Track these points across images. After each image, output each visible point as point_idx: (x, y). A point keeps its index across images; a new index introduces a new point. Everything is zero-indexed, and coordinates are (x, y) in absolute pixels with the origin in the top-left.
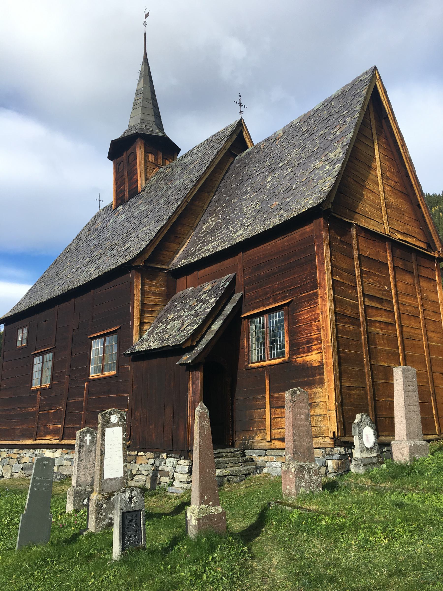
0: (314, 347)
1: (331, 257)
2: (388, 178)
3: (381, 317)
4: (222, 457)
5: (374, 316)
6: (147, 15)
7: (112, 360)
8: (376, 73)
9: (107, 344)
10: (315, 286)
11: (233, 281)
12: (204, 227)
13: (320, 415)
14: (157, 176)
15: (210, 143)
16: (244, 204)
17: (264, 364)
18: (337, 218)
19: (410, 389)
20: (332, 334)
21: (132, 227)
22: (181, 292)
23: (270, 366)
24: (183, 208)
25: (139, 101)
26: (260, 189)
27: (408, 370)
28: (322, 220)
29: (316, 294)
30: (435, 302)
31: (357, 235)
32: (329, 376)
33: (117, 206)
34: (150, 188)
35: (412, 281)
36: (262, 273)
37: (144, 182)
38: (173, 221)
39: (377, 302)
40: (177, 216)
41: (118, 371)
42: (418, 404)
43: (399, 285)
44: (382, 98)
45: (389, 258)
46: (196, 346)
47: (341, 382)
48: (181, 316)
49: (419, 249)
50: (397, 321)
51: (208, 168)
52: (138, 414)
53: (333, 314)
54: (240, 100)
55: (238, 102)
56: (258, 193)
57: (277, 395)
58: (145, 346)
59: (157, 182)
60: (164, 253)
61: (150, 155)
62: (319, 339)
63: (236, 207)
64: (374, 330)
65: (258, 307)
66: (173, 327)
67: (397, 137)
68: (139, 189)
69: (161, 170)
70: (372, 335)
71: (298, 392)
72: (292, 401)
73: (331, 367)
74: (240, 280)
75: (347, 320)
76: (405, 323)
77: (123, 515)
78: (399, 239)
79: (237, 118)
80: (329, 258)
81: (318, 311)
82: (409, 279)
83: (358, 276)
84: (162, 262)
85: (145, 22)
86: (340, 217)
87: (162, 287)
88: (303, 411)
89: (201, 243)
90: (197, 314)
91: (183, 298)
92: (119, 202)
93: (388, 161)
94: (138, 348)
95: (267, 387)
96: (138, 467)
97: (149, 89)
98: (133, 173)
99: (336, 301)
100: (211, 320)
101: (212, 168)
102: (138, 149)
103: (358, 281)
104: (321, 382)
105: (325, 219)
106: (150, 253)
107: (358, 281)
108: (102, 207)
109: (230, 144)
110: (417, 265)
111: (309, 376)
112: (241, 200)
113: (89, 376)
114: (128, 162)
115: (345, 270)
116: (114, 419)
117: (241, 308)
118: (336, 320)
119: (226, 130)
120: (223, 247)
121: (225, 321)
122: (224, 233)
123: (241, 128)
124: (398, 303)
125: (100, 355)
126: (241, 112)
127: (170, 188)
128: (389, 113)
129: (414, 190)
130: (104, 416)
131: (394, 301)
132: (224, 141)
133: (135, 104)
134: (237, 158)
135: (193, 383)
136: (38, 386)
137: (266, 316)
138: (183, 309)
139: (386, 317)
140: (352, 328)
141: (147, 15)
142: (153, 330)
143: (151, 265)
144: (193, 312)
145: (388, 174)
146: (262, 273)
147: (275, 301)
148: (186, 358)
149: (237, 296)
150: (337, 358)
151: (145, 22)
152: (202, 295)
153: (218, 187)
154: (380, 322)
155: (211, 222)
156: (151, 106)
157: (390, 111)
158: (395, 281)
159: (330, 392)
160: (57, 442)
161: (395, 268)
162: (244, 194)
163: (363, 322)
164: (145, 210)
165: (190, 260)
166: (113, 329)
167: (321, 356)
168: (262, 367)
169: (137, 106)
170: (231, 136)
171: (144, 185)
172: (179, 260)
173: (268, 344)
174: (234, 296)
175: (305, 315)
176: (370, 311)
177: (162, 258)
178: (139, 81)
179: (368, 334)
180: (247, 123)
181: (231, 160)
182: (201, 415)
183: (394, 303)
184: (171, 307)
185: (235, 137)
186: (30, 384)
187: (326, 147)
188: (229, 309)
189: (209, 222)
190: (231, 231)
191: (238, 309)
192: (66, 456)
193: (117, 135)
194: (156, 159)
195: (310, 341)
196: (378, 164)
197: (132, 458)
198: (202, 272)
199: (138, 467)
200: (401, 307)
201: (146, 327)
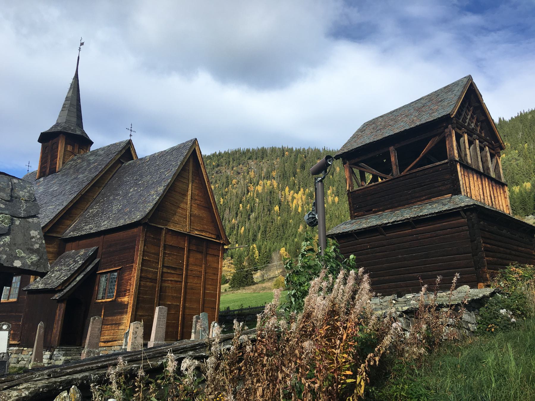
1: (144, 246)
2: (196, 200)
4: (71, 351)
5: (168, 277)
10: (133, 262)
15: (108, 150)
16: (115, 202)
17: (103, 301)
19: (162, 317)
23: (106, 302)
25: (67, 106)
26: (125, 195)
27: (163, 308)
29: (132, 266)
31: (165, 233)
32: (130, 310)
33: (40, 178)
35: (201, 257)
37: (61, 165)
38: (69, 207)
40: (72, 204)
41: (18, 298)
43: (191, 260)
47: (136, 312)
51: (100, 172)
52: (26, 326)
57: (106, 318)
58: (36, 286)
59: (70, 168)
61: (69, 146)
62: (129, 290)
64: (166, 285)
68: (57, 169)
69: (75, 158)
72: (93, 322)
73: (131, 305)
75: (148, 280)
76: (190, 280)
79: (129, 138)
82: (199, 256)
84: (57, 232)
88: (98, 327)
90: (70, 270)
91: (68, 257)
92: (42, 174)
93: (198, 190)
94: (32, 287)
96: (23, 356)
97: (75, 97)
99: (142, 271)
103: (161, 259)
104: (126, 312)
106: (49, 227)
107: (161, 259)
108: (30, 172)
112: (114, 199)
115: (153, 253)
116: (5, 327)
118: (140, 281)
119: (120, 143)
126: (131, 135)
127: (75, 178)
132: (115, 154)
133: (64, 107)
135: (60, 310)
137: (109, 274)
138: (64, 265)
141: (82, 44)
143: (52, 235)
144: (68, 268)
145: (196, 198)
147: (115, 267)
153: (106, 184)
154: (171, 281)
155: (95, 209)
156: (75, 110)
158: (188, 257)
161: (189, 251)
162: (118, 195)
164: (56, 190)
165: (76, 234)
167: (128, 299)
168: (102, 302)
170: (121, 151)
171: (61, 167)
172: (70, 233)
176: (165, 275)
177: (58, 230)
178: (69, 91)
179: (161, 287)
181: (120, 165)
182: (40, 327)
187: (159, 183)
190: (102, 220)
191: (96, 267)
193: (47, 127)
194: (73, 149)
195: (126, 291)
198: (81, 242)
199: (23, 356)
200: (189, 272)
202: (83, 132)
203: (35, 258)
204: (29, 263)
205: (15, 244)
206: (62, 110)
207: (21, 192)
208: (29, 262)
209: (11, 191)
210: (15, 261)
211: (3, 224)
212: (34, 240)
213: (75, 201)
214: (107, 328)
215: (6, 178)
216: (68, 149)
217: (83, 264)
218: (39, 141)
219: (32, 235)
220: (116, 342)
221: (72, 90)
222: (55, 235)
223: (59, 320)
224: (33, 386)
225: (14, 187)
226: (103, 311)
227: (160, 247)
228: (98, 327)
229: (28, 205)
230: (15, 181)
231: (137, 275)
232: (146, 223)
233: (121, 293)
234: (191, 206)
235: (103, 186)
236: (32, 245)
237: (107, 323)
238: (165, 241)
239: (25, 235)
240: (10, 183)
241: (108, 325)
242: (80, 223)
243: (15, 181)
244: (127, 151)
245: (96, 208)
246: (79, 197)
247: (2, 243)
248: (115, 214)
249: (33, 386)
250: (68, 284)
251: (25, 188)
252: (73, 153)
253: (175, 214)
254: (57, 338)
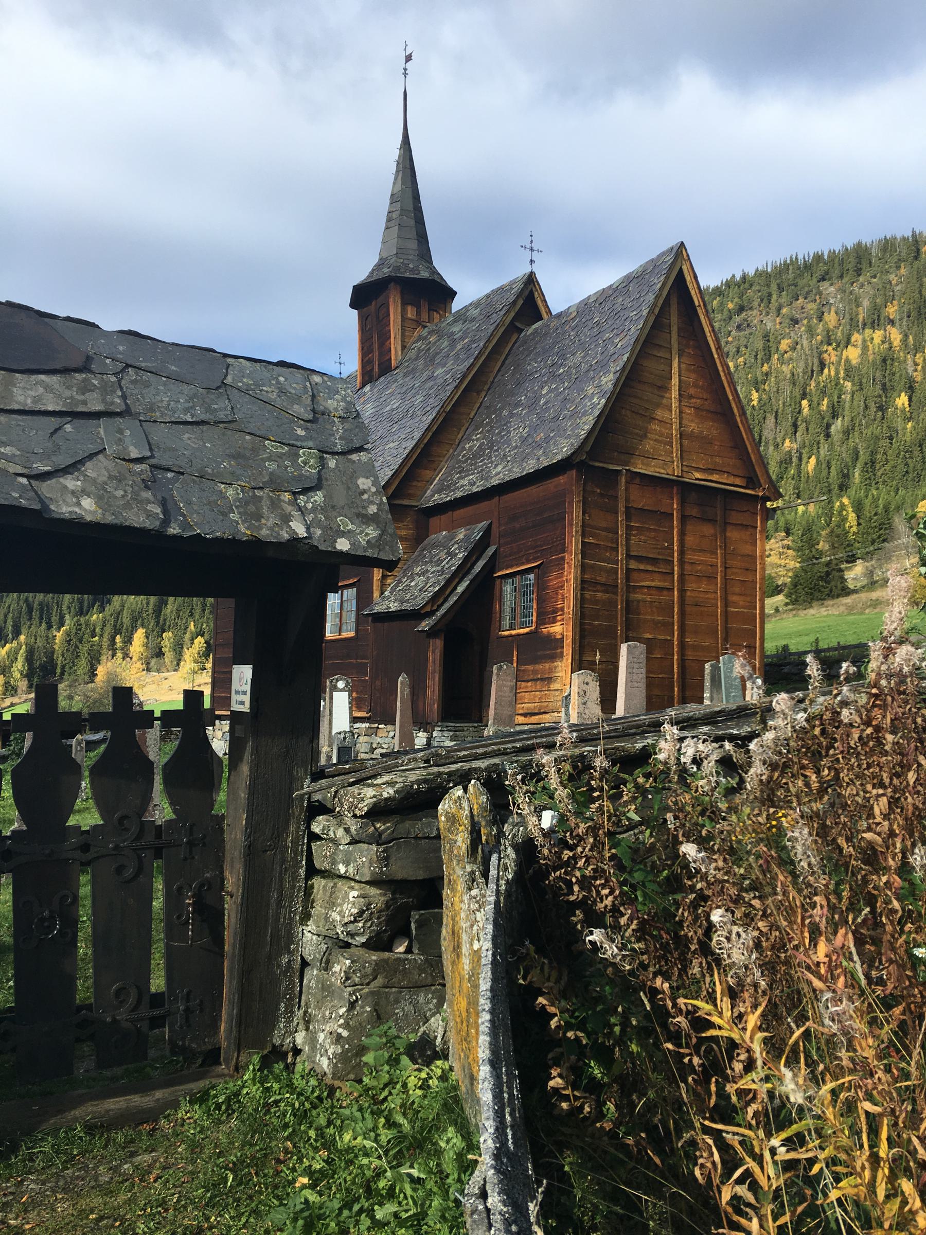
1: (583, 514)
2: (691, 397)
3: (653, 581)
4: (463, 731)
6: (408, 58)
7: (351, 618)
8: (684, 252)
9: (345, 598)
11: (488, 532)
12: (467, 446)
13: (557, 690)
14: (418, 344)
16: (514, 423)
17: (513, 632)
18: (599, 467)
19: (636, 666)
20: (575, 605)
21: (379, 434)
22: (433, 536)
23: (519, 635)
24: (439, 422)
25: (394, 215)
26: (533, 404)
27: (636, 647)
28: (574, 472)
29: (563, 558)
30: (748, 555)
31: (626, 482)
32: (568, 650)
33: (363, 385)
34: (408, 367)
35: (712, 531)
37: (400, 353)
38: (425, 441)
39: (648, 564)
40: (430, 434)
41: (357, 631)
42: (644, 680)
43: (690, 540)
44: (690, 287)
45: (675, 506)
46: (437, 610)
47: (581, 655)
48: (427, 571)
49: (732, 488)
50: (676, 584)
51: (477, 358)
52: (378, 683)
53: (579, 582)
54: (532, 242)
55: (528, 246)
56: (532, 408)
57: (523, 668)
58: (385, 607)
60: (415, 483)
61: (409, 308)
62: (562, 609)
63: (505, 425)
64: (639, 596)
65: (511, 567)
66: (416, 585)
67: (709, 339)
69: (425, 332)
70: (635, 603)
71: (505, 667)
72: (498, 675)
73: (570, 640)
75: (599, 587)
76: (691, 586)
77: (339, 749)
78: (697, 479)
79: (528, 270)
80: (580, 518)
81: (564, 579)
82: (708, 530)
83: (622, 535)
84: (410, 496)
85: (405, 69)
86: (601, 465)
87: (410, 529)
88: (509, 684)
89: (460, 472)
90: (442, 572)
91: (434, 546)
96: (379, 740)
97: (409, 193)
98: (385, 337)
99: (584, 567)
100: (457, 580)
101: (483, 358)
102: (391, 300)
103: (622, 541)
104: (561, 656)
105: (578, 471)
107: (622, 541)
109: (513, 314)
110: (726, 509)
111: (552, 647)
112: (511, 415)
114: (378, 317)
116: (341, 684)
117: (495, 565)
118: (583, 589)
120: (478, 487)
121: (472, 581)
122: (485, 464)
123: (532, 285)
124: (682, 562)
125: (338, 611)
126: (531, 261)
128: (699, 306)
129: (731, 408)
130: (331, 682)
131: (676, 560)
133: (389, 220)
134: (523, 333)
138: (431, 561)
139: (660, 581)
140: (606, 596)
141: (408, 58)
142: (397, 586)
145: (692, 391)
147: (528, 562)
148: (425, 625)
149: (491, 550)
150: (578, 630)
151: (405, 69)
152: (453, 545)
153: (492, 382)
154: (648, 587)
156: (412, 223)
157: (702, 304)
158: (682, 534)
159: (567, 666)
161: (684, 519)
162: (518, 405)
163: (622, 589)
164: (397, 408)
166: (351, 581)
168: (511, 636)
169: (391, 224)
171: (400, 357)
173: (518, 611)
176: (635, 575)
178: (396, 179)
179: (628, 602)
180: (540, 277)
183: (676, 563)
184: (419, 555)
185: (521, 302)
187: (603, 366)
188: (478, 568)
189: (473, 440)
193: (361, 272)
194: (419, 313)
195: (555, 611)
196: (675, 381)
197: (373, 731)
199: (379, 740)
200: (687, 567)
201: (389, 581)
202: (434, 271)
203: (372, 532)
204: (364, 543)
205: (333, 507)
206: (387, 228)
207: (330, 401)
208: (362, 540)
209: (312, 400)
210: (338, 540)
211: (307, 468)
212: (365, 496)
213: (435, 427)
214: (526, 687)
215: (298, 374)
216: (409, 315)
217: (466, 559)
218: (353, 305)
219: (361, 487)
220: (548, 716)
221: (400, 177)
222: (406, 502)
223: (434, 672)
224: (401, 780)
225: (315, 392)
226: (515, 653)
227: (617, 513)
228: (509, 684)
229: (347, 426)
230: (317, 379)
231: (576, 578)
232: (582, 463)
233: (547, 615)
234: (681, 412)
235: (486, 388)
236: (365, 508)
237: (526, 678)
238: (627, 500)
239: (349, 488)
240: (308, 384)
241: (528, 681)
242: (449, 474)
243: (317, 379)
244: (527, 301)
245: (477, 440)
246: (441, 419)
247: (311, 505)
248: (516, 447)
249: (401, 780)
250: (441, 600)
251: (337, 392)
252: (419, 323)
253: (645, 436)
254: (436, 706)
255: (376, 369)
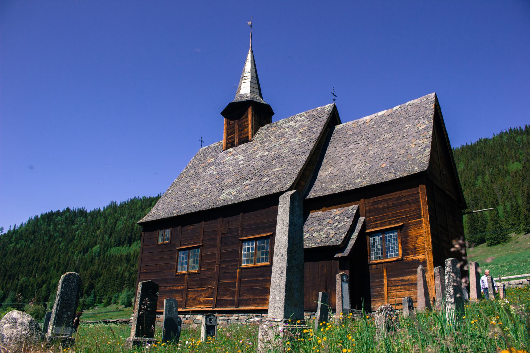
0: (421, 251)
33: (227, 148)
36: (380, 206)
74: (362, 211)
92: (229, 145)
95: (385, 274)
113: (241, 265)
126: (334, 100)
136: (185, 271)
146: (380, 206)
149: (362, 219)
160: (211, 309)
166: (266, 235)
174: (360, 218)
175: (413, 232)
186: (175, 270)
188: (359, 227)
192: (221, 318)
255: (237, 141)
